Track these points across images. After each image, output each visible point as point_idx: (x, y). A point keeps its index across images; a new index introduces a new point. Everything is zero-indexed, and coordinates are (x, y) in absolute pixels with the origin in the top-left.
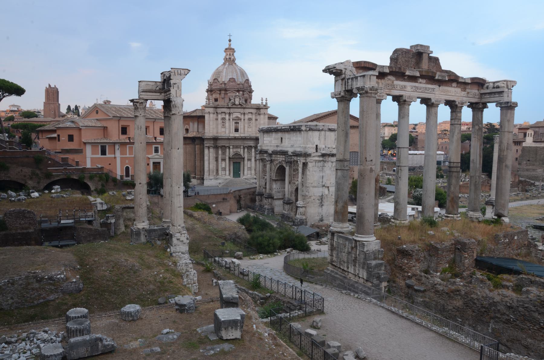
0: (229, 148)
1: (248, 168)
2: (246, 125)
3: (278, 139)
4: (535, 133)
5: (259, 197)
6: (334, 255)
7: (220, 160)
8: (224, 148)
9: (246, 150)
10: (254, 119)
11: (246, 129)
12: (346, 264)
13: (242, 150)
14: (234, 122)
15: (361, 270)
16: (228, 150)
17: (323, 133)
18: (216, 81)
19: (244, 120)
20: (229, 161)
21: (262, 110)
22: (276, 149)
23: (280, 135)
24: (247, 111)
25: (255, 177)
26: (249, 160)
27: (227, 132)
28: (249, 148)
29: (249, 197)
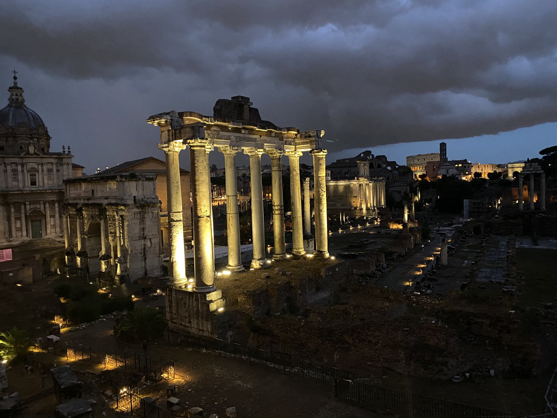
0: (25, 205)
1: (51, 225)
7: (13, 219)
8: (18, 206)
9: (47, 205)
10: (55, 170)
11: (46, 182)
13: (42, 206)
14: (29, 174)
15: (205, 322)
16: (23, 206)
17: (140, 183)
19: (42, 171)
22: (86, 202)
24: (45, 161)
26: (53, 216)
27: (21, 185)
28: (52, 203)
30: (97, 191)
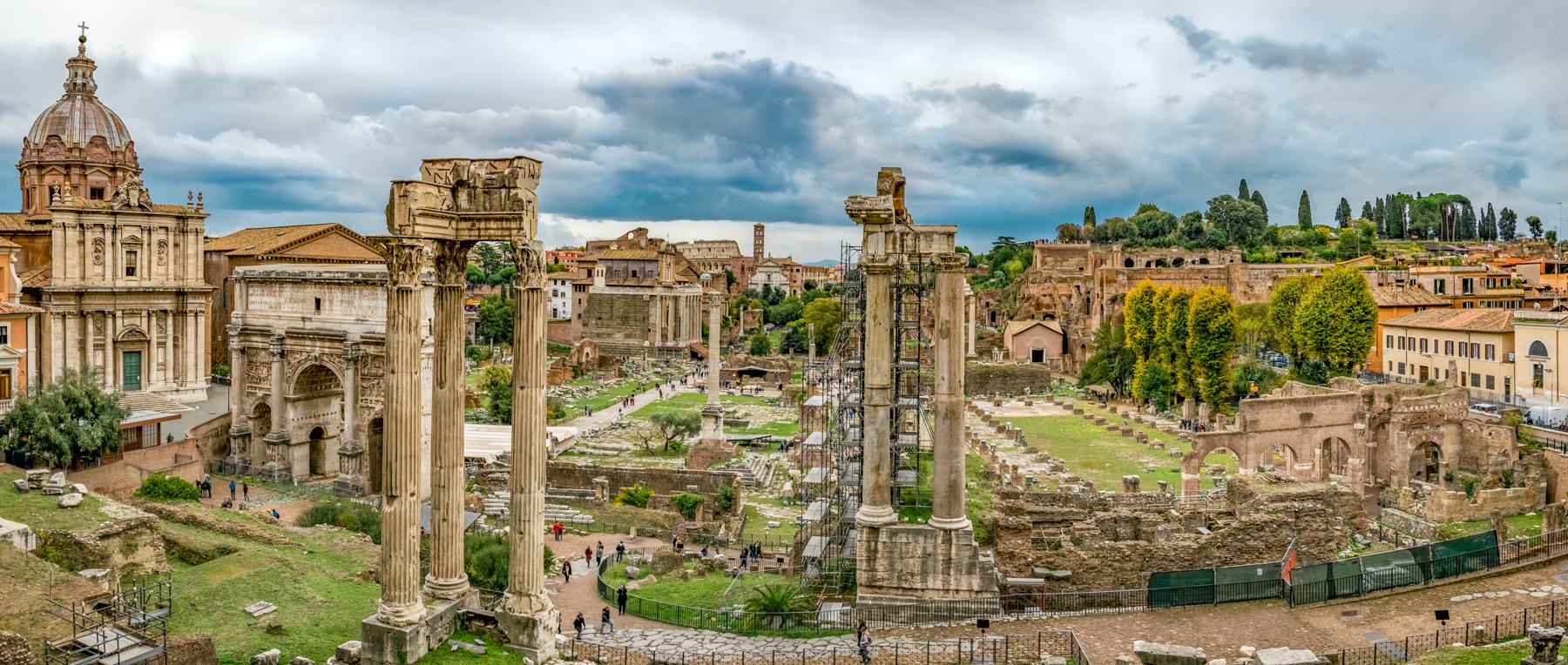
0: (114, 316)
2: (154, 259)
3: (304, 301)
4: (609, 269)
5: (240, 441)
6: (881, 568)
7: (90, 348)
9: (154, 320)
11: (154, 269)
12: (918, 578)
13: (145, 320)
16: (110, 321)
18: (54, 141)
20: (115, 348)
21: (190, 222)
22: (299, 324)
23: (311, 292)
24: (156, 222)
25: (175, 386)
26: (162, 345)
27: (109, 274)
29: (210, 442)
30: (331, 302)
